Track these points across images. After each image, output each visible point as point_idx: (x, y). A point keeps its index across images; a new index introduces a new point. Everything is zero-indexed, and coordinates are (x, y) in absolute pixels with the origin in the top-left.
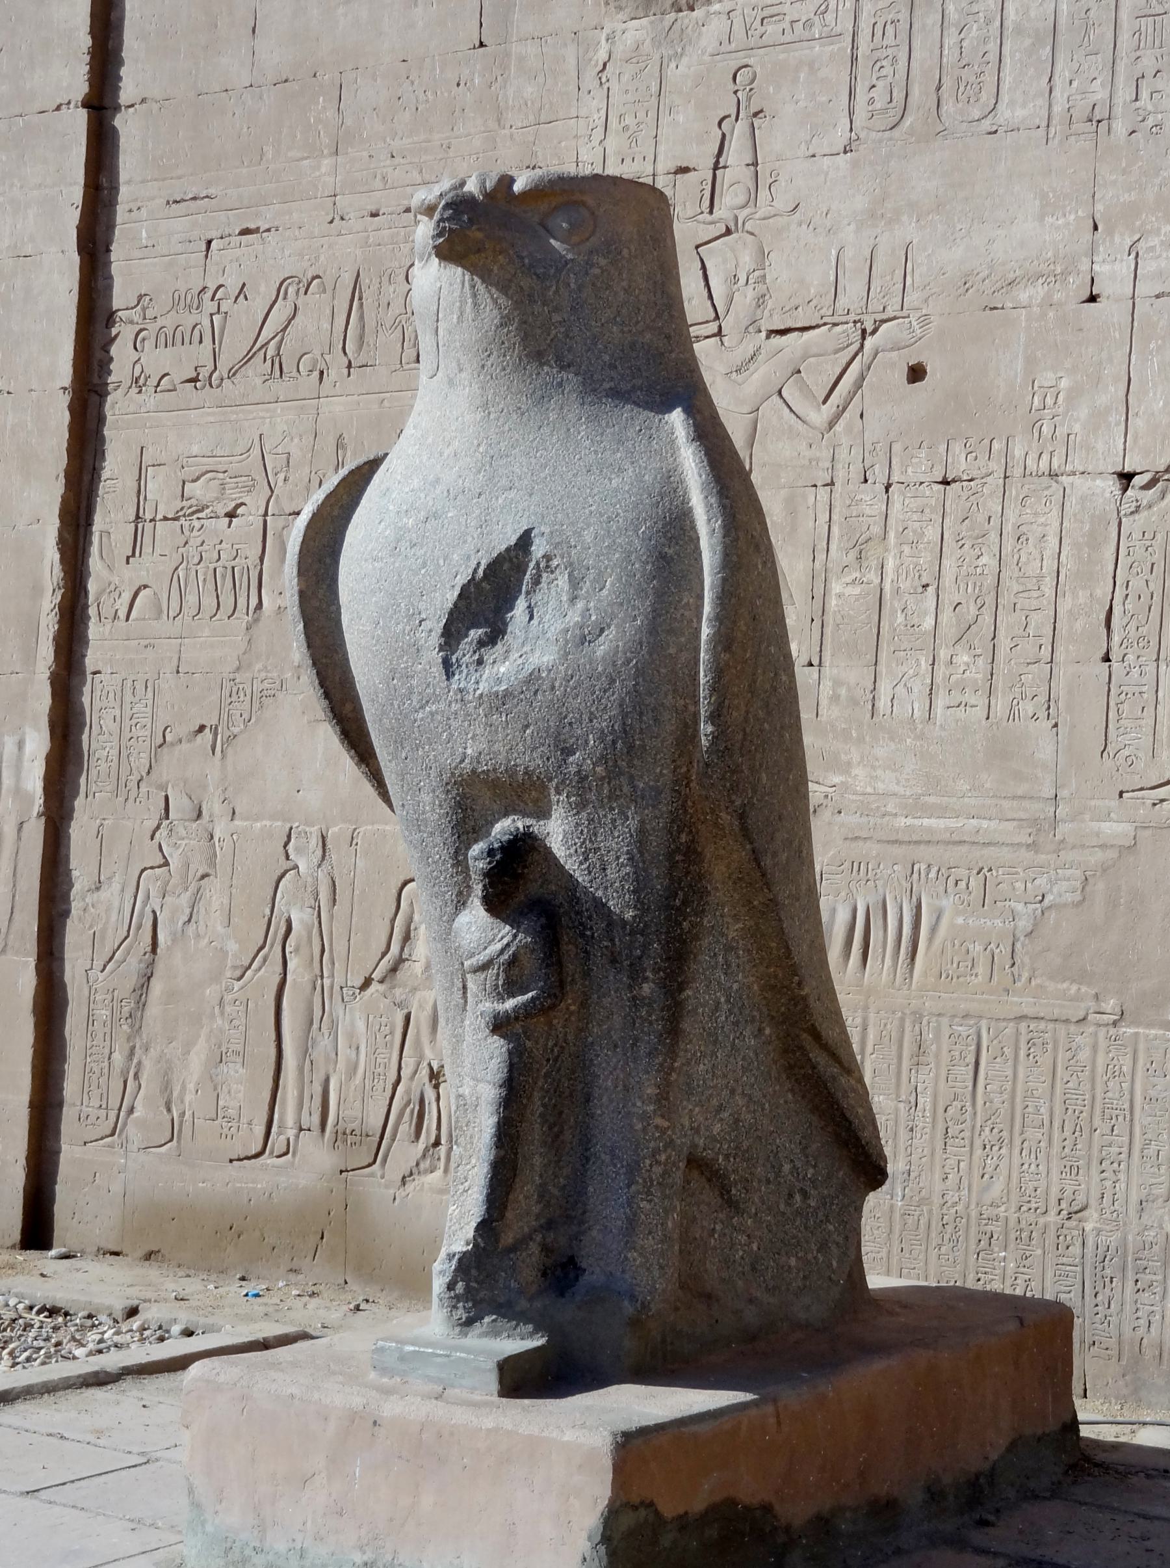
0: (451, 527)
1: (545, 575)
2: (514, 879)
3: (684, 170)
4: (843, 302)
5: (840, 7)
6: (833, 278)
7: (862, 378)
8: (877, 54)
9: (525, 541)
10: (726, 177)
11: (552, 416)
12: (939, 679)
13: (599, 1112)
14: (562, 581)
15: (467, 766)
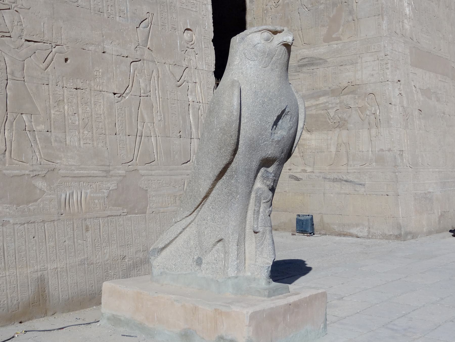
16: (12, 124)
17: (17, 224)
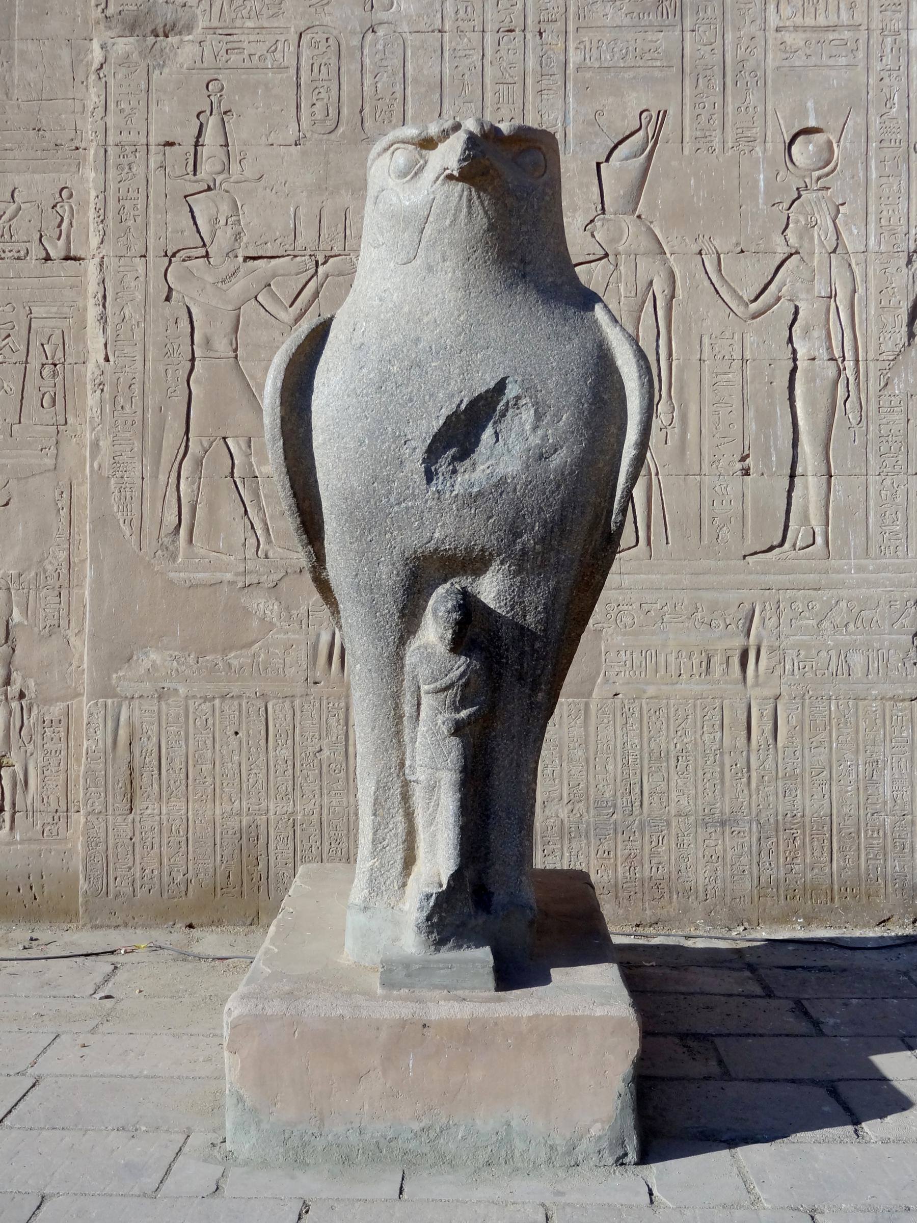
0: (435, 373)
1: (511, 411)
3: (171, 144)
4: (301, 241)
5: (286, 50)
6: (292, 226)
7: (316, 294)
8: (315, 84)
9: (501, 386)
10: (204, 152)
11: (519, 298)
13: (497, 783)
14: (527, 415)
15: (432, 546)
16: (199, 463)
17: (194, 697)
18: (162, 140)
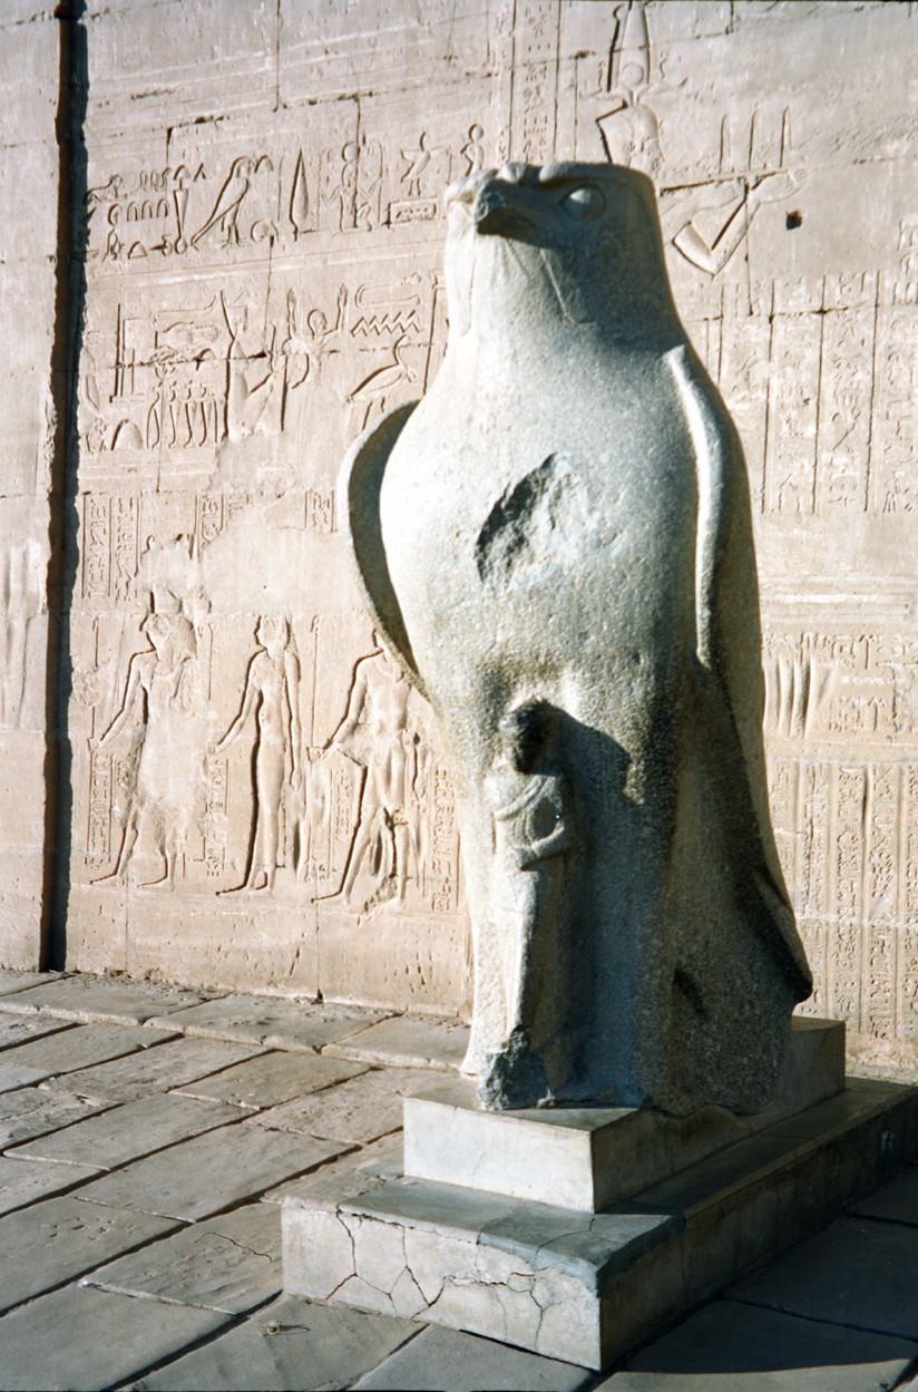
2: (544, 740)
3: (582, 55)
4: (729, 161)
12: (820, 479)
14: (582, 496)
18: (574, 51)
